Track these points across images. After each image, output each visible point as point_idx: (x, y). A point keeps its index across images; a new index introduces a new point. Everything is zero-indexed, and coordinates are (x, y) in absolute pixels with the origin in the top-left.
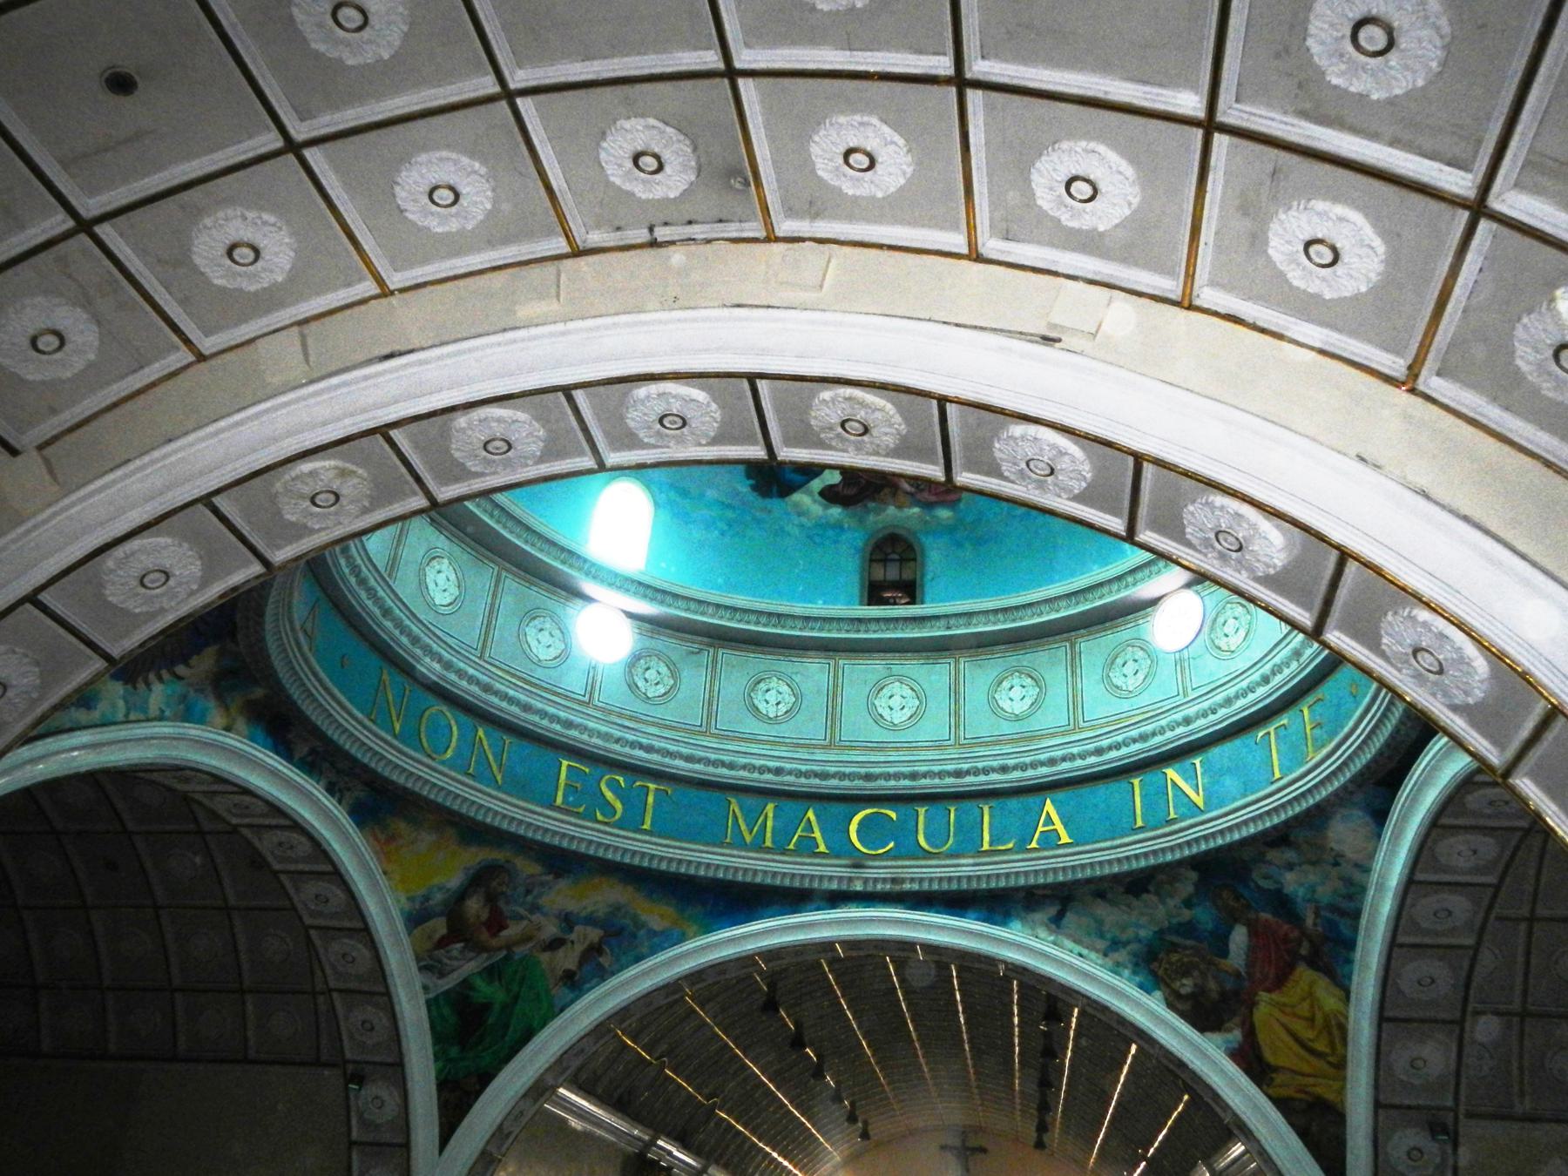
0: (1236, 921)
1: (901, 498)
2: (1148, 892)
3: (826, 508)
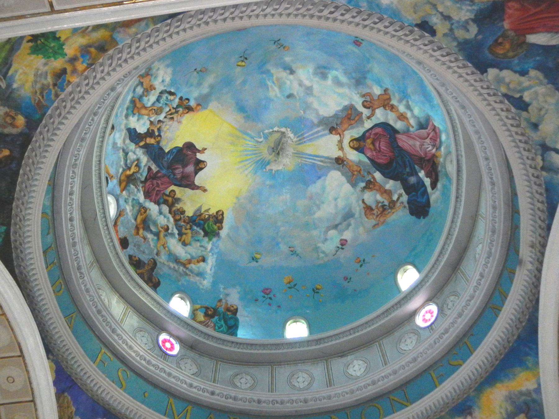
0: (524, 42)
1: (437, 154)
2: (521, 97)
3: (437, 189)
